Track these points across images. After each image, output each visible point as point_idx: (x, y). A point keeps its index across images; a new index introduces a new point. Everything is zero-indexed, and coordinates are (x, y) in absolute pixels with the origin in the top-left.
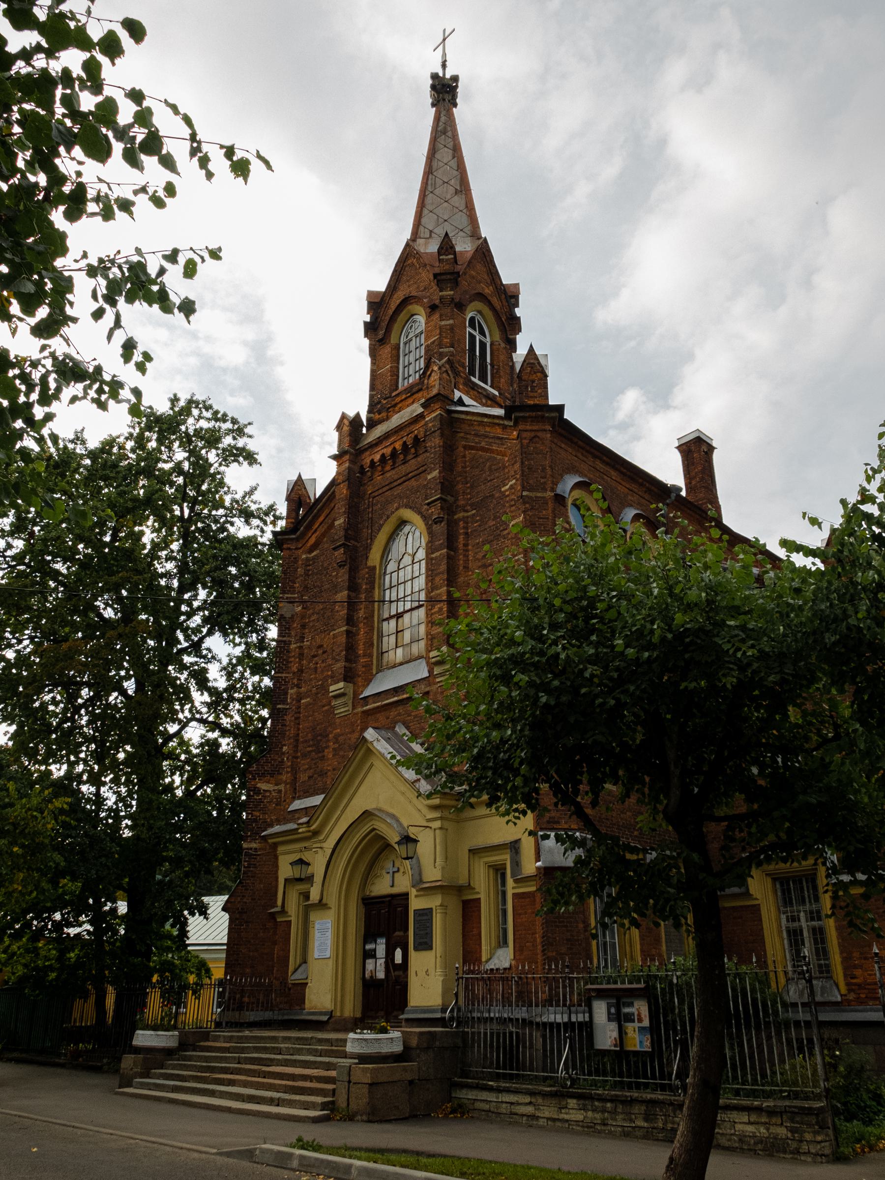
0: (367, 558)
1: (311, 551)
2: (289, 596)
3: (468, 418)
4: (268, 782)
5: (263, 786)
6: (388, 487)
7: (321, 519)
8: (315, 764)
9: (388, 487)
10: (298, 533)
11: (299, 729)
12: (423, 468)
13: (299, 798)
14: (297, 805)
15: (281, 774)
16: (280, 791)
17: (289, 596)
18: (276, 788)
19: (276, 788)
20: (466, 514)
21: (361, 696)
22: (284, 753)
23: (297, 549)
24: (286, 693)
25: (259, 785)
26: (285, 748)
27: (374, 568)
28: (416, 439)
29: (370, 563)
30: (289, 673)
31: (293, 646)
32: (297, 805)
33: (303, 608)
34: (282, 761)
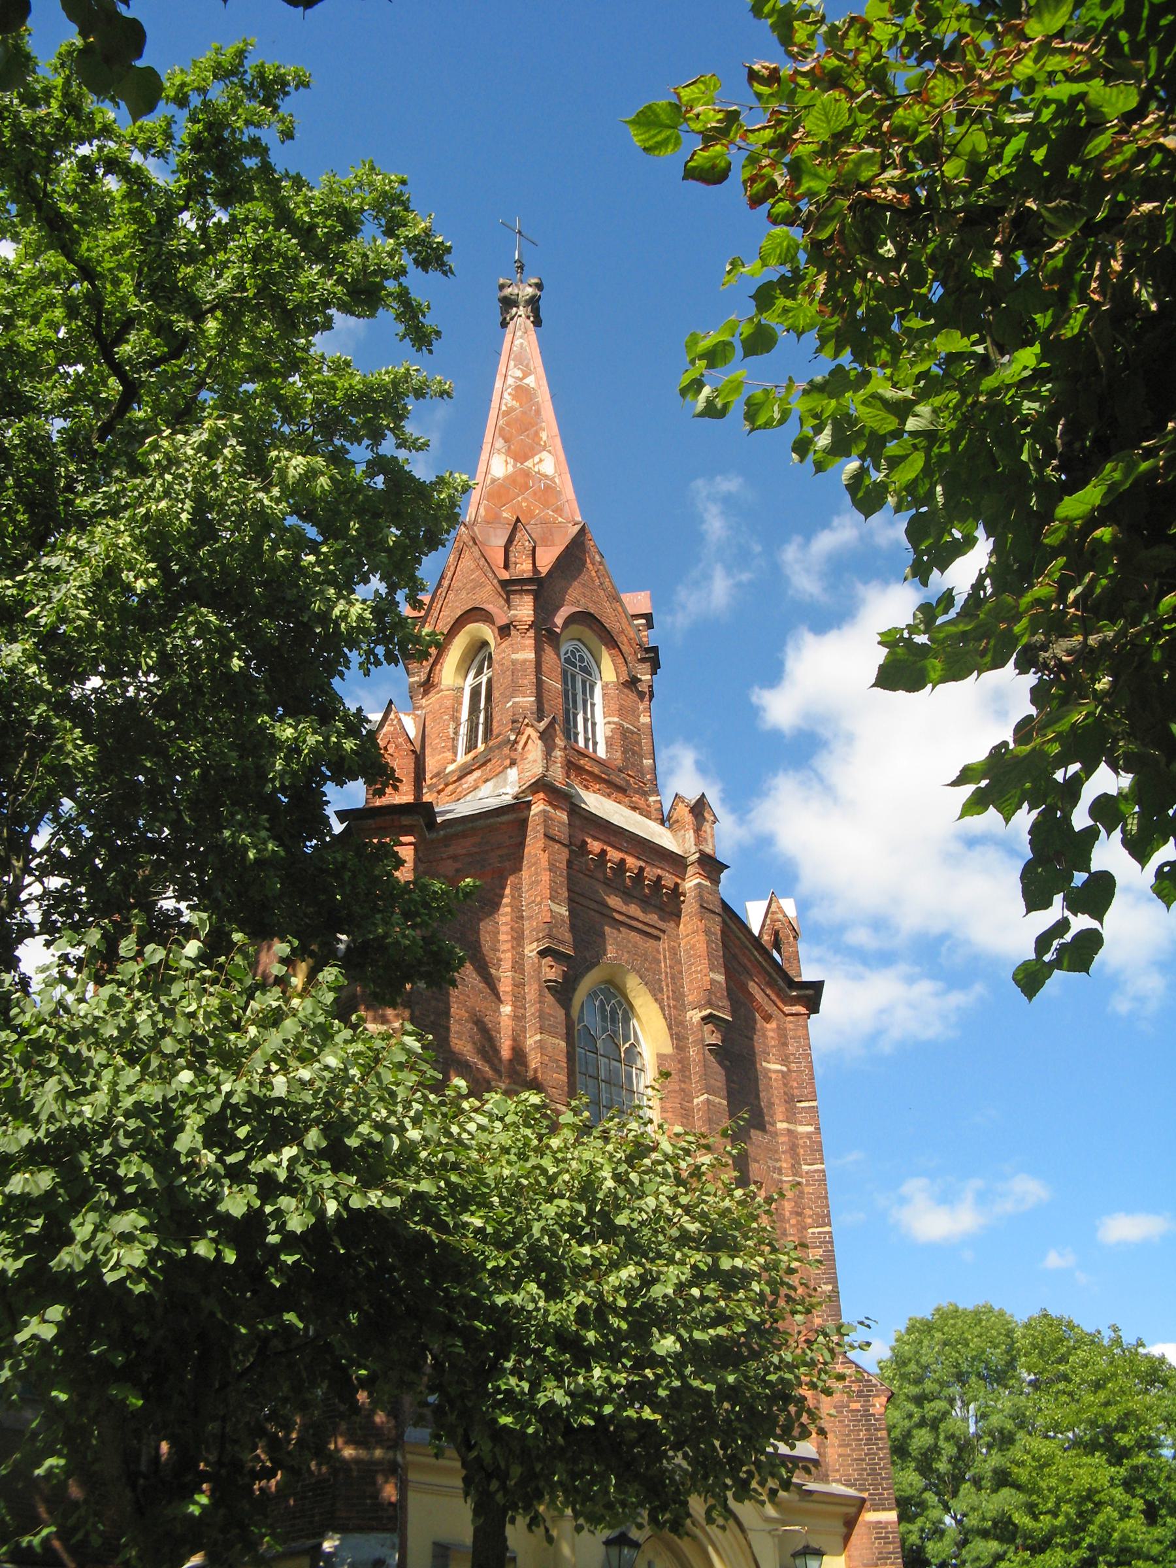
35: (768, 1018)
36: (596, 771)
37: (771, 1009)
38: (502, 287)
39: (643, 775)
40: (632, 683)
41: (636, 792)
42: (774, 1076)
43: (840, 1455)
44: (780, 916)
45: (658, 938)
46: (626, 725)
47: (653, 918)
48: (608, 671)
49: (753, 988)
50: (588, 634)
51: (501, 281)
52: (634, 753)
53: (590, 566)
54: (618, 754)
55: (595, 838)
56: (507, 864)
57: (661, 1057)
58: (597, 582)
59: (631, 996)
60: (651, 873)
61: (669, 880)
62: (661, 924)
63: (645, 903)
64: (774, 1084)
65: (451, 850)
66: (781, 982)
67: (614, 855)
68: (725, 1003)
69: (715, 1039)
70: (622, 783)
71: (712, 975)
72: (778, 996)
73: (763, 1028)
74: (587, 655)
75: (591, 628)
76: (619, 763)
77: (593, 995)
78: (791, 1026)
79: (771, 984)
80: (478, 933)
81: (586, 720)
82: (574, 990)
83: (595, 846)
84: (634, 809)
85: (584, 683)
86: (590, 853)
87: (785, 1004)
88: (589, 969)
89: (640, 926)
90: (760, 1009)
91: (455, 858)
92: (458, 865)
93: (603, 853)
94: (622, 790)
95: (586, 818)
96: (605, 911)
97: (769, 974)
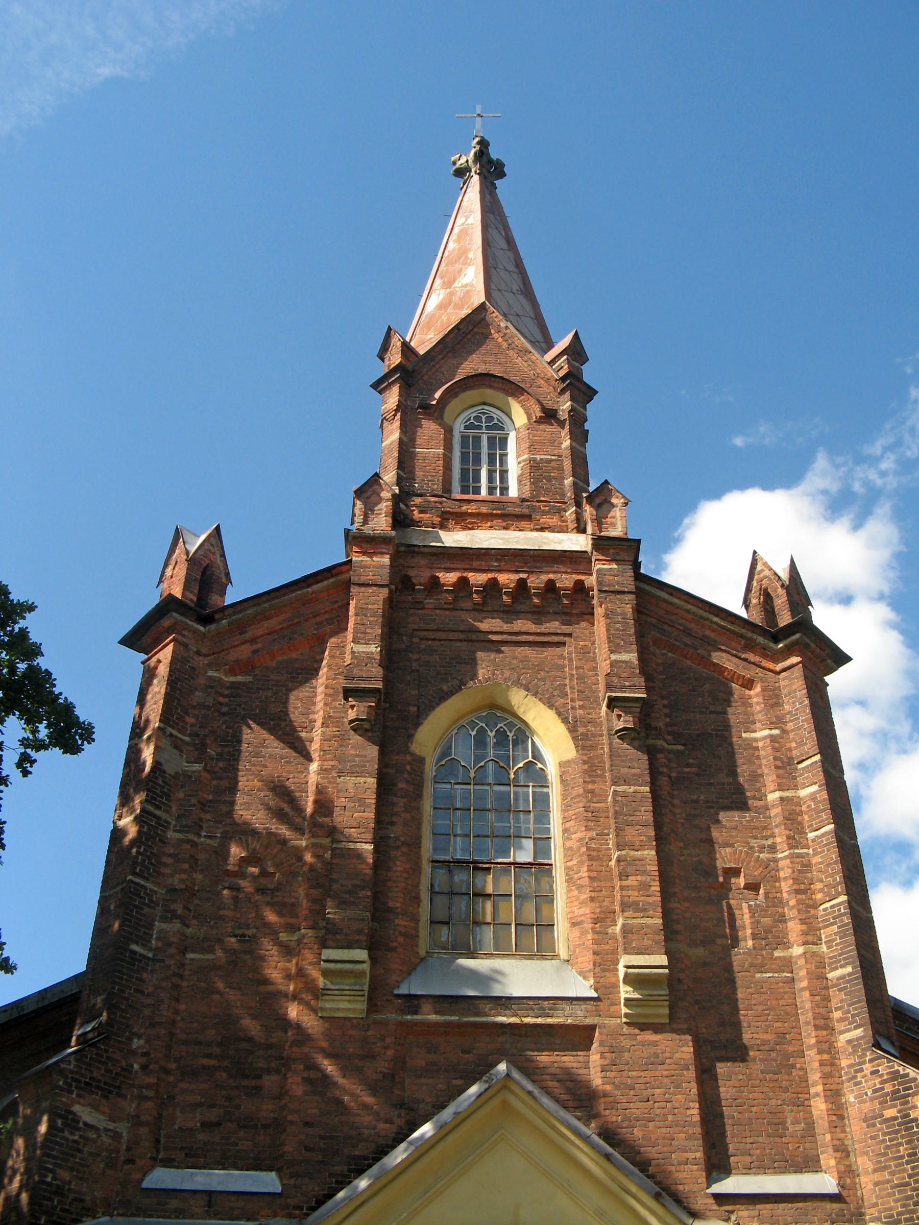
0: (411, 736)
1: (232, 672)
2: (175, 732)
3: (675, 600)
4: (96, 1108)
5: (85, 1113)
6: (462, 636)
7: (273, 623)
8: (229, 1099)
9: (462, 636)
10: (213, 627)
11: (176, 1012)
12: (561, 639)
13: (168, 1163)
14: (161, 1177)
15: (124, 1097)
16: (117, 1136)
17: (175, 732)
18: (111, 1126)
19: (111, 1126)
20: (666, 745)
21: (403, 990)
22: (133, 1053)
23: (198, 653)
24: (151, 926)
25: (77, 1108)
26: (136, 1043)
27: (421, 761)
28: (580, 589)
29: (415, 748)
30: (158, 885)
31: (170, 834)
32: (161, 1177)
33: (205, 769)
34: (128, 1069)
35: (749, 684)
36: (484, 510)
37: (748, 672)
38: (454, 163)
39: (563, 495)
40: (549, 416)
41: (544, 513)
42: (760, 744)
43: (876, 1184)
44: (767, 572)
45: (564, 644)
46: (538, 457)
47: (554, 626)
48: (519, 416)
49: (718, 658)
50: (489, 394)
51: (453, 159)
52: (549, 479)
53: (496, 336)
54: (527, 488)
55: (448, 570)
56: (327, 629)
57: (563, 765)
58: (505, 345)
59: (520, 713)
60: (536, 581)
61: (565, 580)
62: (566, 629)
63: (538, 614)
64: (762, 753)
65: (248, 635)
66: (760, 640)
67: (478, 579)
68: (641, 681)
69: (624, 722)
70: (526, 511)
71: (613, 657)
72: (764, 656)
73: (742, 697)
74: (496, 414)
75: (491, 387)
76: (527, 495)
77: (459, 725)
78: (786, 682)
79: (750, 646)
80: (286, 702)
81: (491, 473)
82: (418, 725)
83: (449, 578)
84: (542, 529)
85: (491, 440)
86: (444, 585)
87: (776, 661)
88: (444, 697)
89: (531, 638)
90: (734, 677)
91: (253, 641)
92: (255, 647)
93: (463, 581)
94: (528, 517)
95: (432, 554)
96: (481, 637)
97: (742, 636)
